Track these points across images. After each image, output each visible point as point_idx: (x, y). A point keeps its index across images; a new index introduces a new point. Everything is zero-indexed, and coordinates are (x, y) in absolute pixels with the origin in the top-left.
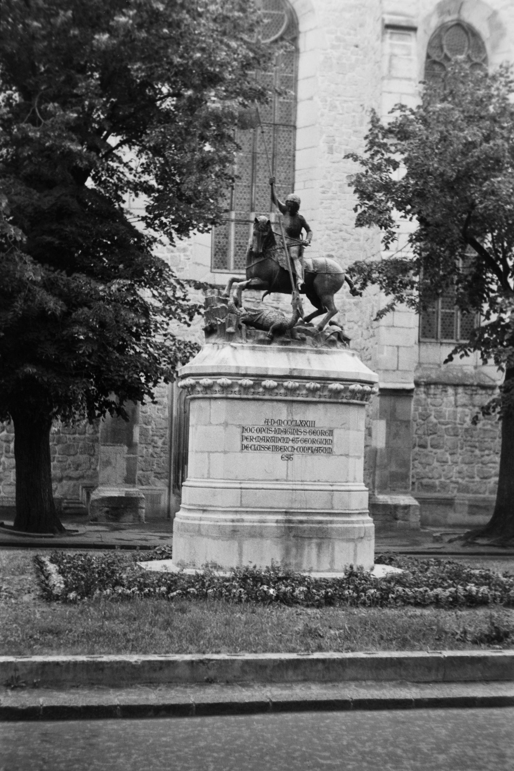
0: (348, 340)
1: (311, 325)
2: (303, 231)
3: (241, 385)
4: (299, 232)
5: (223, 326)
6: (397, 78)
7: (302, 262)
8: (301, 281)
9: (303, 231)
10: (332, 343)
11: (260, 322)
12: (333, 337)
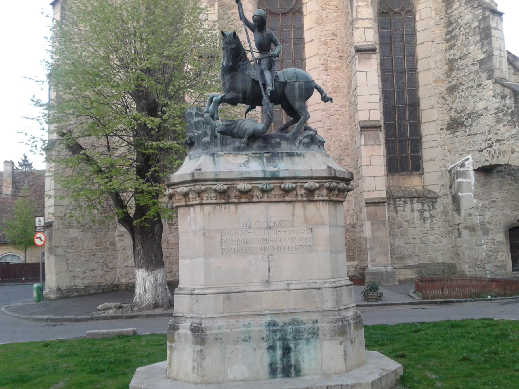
0: (322, 143)
2: (273, 45)
3: (215, 191)
5: (200, 136)
8: (269, 88)
9: (273, 45)
10: (307, 145)
11: (235, 131)
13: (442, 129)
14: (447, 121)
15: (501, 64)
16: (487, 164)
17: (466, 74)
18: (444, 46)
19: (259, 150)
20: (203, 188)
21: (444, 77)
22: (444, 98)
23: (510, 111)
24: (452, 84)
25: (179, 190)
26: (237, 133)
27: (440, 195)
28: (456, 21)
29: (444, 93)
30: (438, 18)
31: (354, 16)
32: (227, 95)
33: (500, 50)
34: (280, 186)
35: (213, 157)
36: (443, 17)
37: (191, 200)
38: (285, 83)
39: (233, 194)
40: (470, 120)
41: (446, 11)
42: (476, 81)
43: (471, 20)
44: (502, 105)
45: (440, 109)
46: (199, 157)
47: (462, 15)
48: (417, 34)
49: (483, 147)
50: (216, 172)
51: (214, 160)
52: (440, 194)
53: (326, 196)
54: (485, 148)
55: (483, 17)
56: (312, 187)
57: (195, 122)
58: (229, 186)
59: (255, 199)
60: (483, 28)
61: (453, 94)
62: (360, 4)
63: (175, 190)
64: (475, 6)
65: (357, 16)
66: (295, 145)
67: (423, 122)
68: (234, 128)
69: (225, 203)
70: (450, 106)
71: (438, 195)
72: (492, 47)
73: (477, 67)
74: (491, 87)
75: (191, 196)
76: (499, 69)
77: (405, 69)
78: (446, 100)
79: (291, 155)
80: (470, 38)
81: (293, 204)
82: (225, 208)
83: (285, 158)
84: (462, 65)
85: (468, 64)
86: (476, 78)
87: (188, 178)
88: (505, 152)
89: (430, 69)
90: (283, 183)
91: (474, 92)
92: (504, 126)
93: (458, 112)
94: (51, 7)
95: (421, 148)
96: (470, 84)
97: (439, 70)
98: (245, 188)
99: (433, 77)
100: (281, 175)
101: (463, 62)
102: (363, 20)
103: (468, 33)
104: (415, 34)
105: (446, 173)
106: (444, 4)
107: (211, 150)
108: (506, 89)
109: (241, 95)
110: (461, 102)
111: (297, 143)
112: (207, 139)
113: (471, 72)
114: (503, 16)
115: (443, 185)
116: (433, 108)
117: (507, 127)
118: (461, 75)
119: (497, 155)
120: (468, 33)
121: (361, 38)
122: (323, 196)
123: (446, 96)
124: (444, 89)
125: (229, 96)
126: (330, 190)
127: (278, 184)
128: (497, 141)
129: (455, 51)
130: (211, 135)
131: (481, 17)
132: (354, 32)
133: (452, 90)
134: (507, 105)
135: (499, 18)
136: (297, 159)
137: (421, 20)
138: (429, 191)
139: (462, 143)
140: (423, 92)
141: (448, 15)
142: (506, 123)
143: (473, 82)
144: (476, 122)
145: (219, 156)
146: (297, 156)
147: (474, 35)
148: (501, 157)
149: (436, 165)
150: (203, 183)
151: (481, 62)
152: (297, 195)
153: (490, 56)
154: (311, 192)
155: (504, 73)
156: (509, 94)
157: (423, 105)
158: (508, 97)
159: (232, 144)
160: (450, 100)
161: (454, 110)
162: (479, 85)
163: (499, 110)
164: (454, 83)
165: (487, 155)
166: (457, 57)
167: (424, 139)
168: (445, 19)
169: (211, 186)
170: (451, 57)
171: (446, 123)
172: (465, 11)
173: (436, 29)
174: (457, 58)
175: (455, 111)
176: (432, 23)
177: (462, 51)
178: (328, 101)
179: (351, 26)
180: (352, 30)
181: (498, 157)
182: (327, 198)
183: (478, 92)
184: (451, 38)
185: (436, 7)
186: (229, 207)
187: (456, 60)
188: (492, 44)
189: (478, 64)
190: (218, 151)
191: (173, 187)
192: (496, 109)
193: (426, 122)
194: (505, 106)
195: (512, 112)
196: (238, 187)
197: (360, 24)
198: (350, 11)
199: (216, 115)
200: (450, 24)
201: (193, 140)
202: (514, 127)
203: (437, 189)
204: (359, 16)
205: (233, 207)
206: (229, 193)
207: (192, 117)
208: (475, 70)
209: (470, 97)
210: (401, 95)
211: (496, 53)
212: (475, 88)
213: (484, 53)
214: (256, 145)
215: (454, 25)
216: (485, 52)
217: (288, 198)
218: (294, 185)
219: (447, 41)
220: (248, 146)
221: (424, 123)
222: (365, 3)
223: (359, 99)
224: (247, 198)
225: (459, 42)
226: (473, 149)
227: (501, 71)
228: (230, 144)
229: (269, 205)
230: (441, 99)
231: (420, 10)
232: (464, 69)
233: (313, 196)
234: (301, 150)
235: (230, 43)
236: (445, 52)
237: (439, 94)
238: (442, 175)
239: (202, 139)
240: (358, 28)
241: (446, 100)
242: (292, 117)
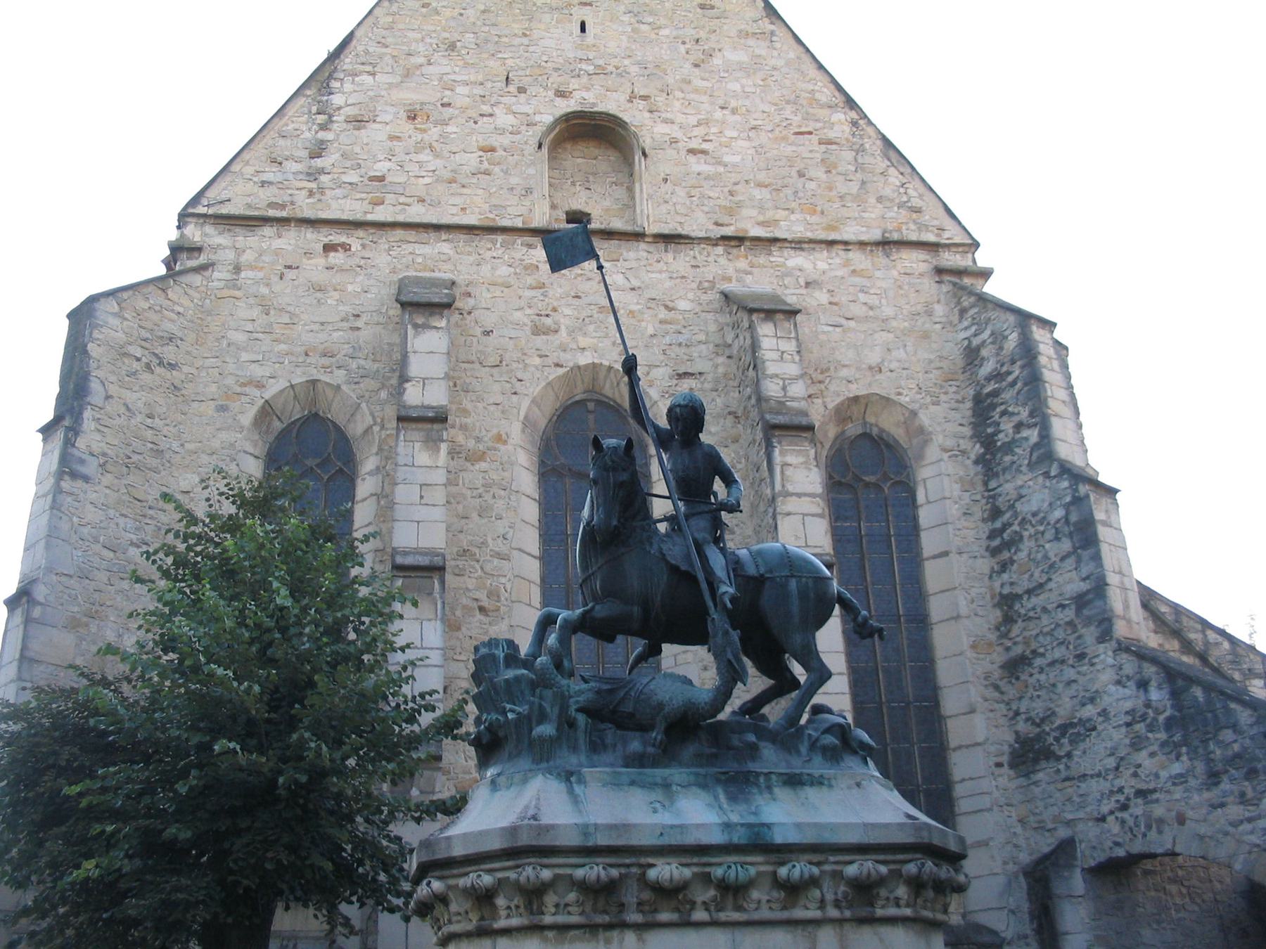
1: (764, 718)
2: (718, 485)
3: (584, 887)
4: (709, 491)
5: (526, 723)
6: (792, 494)
7: (723, 550)
11: (628, 707)
12: (830, 740)
13: (999, 765)
14: (1010, 746)
15: (1126, 606)
16: (1121, 852)
17: (1045, 630)
18: (985, 564)
19: (701, 766)
20: (546, 874)
21: (992, 637)
22: (997, 687)
23: (1161, 718)
24: (1012, 654)
25: (462, 882)
26: (632, 715)
27: (1009, 937)
28: (1012, 507)
29: (996, 675)
30: (968, 501)
31: (778, 487)
32: (598, 607)
33: (1120, 573)
34: (775, 873)
35: (568, 780)
36: (978, 497)
37: (503, 913)
38: (759, 581)
39: (631, 895)
40: (1065, 741)
41: (986, 484)
42: (1071, 647)
43: (1046, 504)
44: (1140, 702)
45: (991, 715)
46: (525, 781)
47: (1024, 492)
48: (923, 535)
49: (1105, 809)
50: (586, 826)
51: (571, 791)
52: (1008, 935)
53: (908, 905)
54: (1112, 812)
55: (1074, 497)
56: (869, 874)
57: (507, 681)
58: (623, 871)
59: (700, 915)
60: (1075, 524)
61: (1018, 678)
62: (790, 459)
63: (452, 882)
64: (1053, 474)
65: (783, 486)
66: (798, 752)
67: (953, 744)
68: (623, 699)
69: (610, 927)
70: (1014, 707)
71: (1004, 939)
72: (1102, 566)
73: (1069, 614)
74: (1110, 661)
75: (501, 902)
76: (1124, 618)
77: (900, 616)
78: (1002, 693)
79: (794, 781)
80: (1047, 546)
81: (810, 929)
82: (608, 941)
83: (776, 790)
84: (1034, 609)
85: (1049, 607)
86: (1071, 638)
87: (496, 845)
88: (1160, 821)
89: (957, 618)
90: (782, 864)
91: (1070, 673)
92: (1152, 755)
93: (1034, 723)
94: (40, 436)
95: (952, 812)
96: (1057, 654)
97: (978, 620)
98: (671, 880)
99: (969, 636)
100: (779, 839)
101: (1034, 600)
102: (799, 495)
103: (1043, 533)
104: (918, 536)
105: (1017, 877)
106: (979, 468)
107: (559, 762)
108: (1146, 665)
109: (636, 610)
110: (1039, 696)
111: (804, 749)
112: (546, 730)
113: (1058, 625)
114: (1118, 496)
115: (1013, 912)
116: (972, 711)
117: (1161, 757)
118: (1034, 633)
119: (1143, 829)
120: (1043, 533)
121: (797, 537)
122: (898, 906)
123: (1001, 684)
124: (996, 666)
125: (601, 611)
126: (917, 885)
127: (769, 868)
128: (1140, 793)
129: (1015, 576)
130: (560, 716)
131: (1068, 499)
132: (779, 523)
133: (1014, 667)
134: (1154, 704)
135: (1109, 501)
136: (811, 793)
137: (929, 502)
138: (979, 928)
139: (1052, 801)
140: (946, 673)
141: (992, 497)
142: (1155, 748)
143: (1063, 648)
144: (1082, 746)
145: (581, 781)
146: (812, 784)
147: (1057, 539)
148: (1153, 834)
149: (992, 857)
150: (546, 861)
151: (1081, 601)
152: (822, 901)
153: (1100, 587)
154: (864, 890)
155: (1135, 626)
156: (1154, 677)
157: (951, 703)
158: (1154, 683)
159: (619, 746)
160: (1012, 692)
161: (1023, 716)
162: (1081, 657)
163: (1134, 718)
164: (1018, 650)
165: (1116, 829)
166: (1019, 590)
167: (959, 790)
168: (984, 501)
169: (568, 871)
170: (1006, 591)
171: (1006, 748)
172: (1031, 483)
173: (966, 524)
174: (1020, 592)
175: (1027, 720)
176: (954, 510)
177: (1032, 575)
178: (871, 635)
179: (771, 510)
180: (774, 518)
181: (1144, 835)
182: (908, 912)
183: (1079, 673)
184: (1001, 544)
185: (962, 473)
186: (621, 941)
187: (1018, 597)
188: (1100, 558)
189: (1073, 607)
190: (581, 765)
191: (446, 873)
192: (1127, 713)
193: (960, 747)
194: (1148, 705)
195: (1169, 719)
196: (652, 874)
197: (791, 505)
198: (766, 474)
199: (566, 663)
200: (995, 513)
201: (501, 734)
202: (1178, 758)
204: (790, 488)
205: (630, 937)
207: (497, 667)
208: (1067, 619)
209: (1060, 686)
211: (1112, 579)
212: (1071, 662)
213: (1084, 580)
214: (689, 750)
215: (1007, 515)
216: (1087, 578)
217: (798, 913)
218: (815, 870)
219: (994, 552)
220: (666, 754)
221: (954, 750)
222: (801, 459)
224: (677, 910)
225: (1022, 555)
226: (1081, 815)
227: (1129, 621)
228: (615, 745)
229: (739, 934)
230: (991, 689)
231: (924, 480)
232: (1039, 618)
233: (873, 906)
234: (818, 767)
235: (614, 469)
236: (990, 577)
237: (986, 678)
238: (1010, 882)
239: (531, 730)
240: (789, 514)
241: (1002, 693)
242: (770, 677)
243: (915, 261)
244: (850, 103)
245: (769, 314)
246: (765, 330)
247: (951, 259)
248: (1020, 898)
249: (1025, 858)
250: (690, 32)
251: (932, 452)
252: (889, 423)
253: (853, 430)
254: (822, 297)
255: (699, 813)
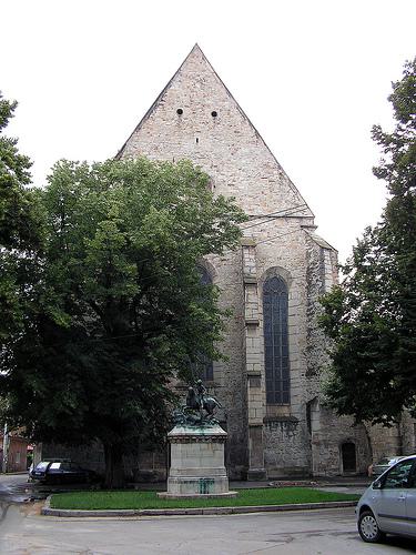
133: (309, 348)
197: (250, 306)
200: (309, 304)
203: (299, 417)
206: (187, 439)
210: (277, 349)
223: (247, 356)
243: (295, 223)
244: (280, 167)
245: (247, 247)
246: (246, 251)
247: (305, 222)
248: (304, 411)
249: (307, 401)
250: (231, 142)
251: (294, 284)
252: (283, 275)
253: (272, 276)
254: (265, 235)
255: (197, 432)
